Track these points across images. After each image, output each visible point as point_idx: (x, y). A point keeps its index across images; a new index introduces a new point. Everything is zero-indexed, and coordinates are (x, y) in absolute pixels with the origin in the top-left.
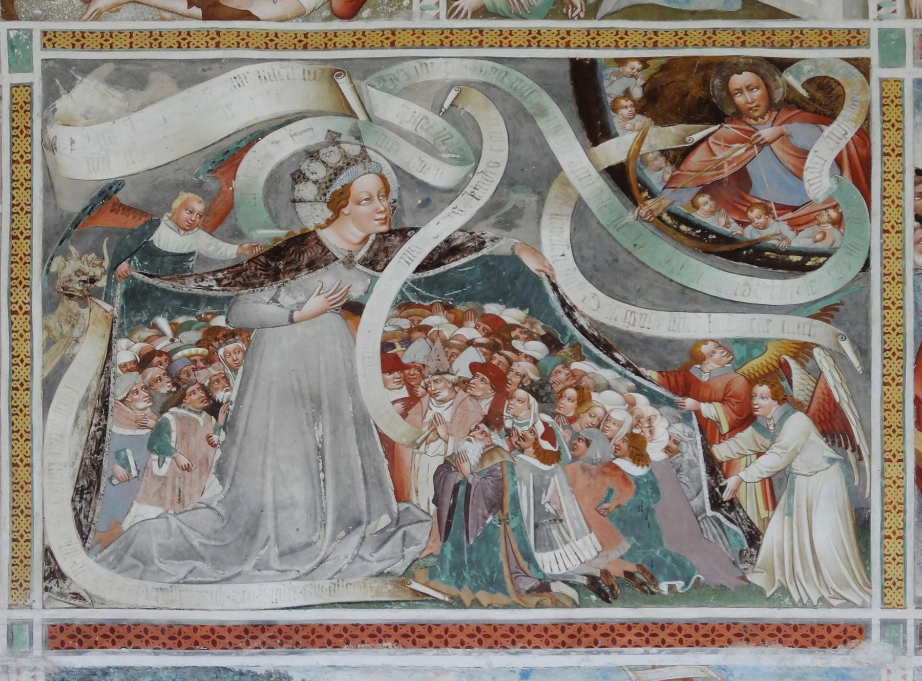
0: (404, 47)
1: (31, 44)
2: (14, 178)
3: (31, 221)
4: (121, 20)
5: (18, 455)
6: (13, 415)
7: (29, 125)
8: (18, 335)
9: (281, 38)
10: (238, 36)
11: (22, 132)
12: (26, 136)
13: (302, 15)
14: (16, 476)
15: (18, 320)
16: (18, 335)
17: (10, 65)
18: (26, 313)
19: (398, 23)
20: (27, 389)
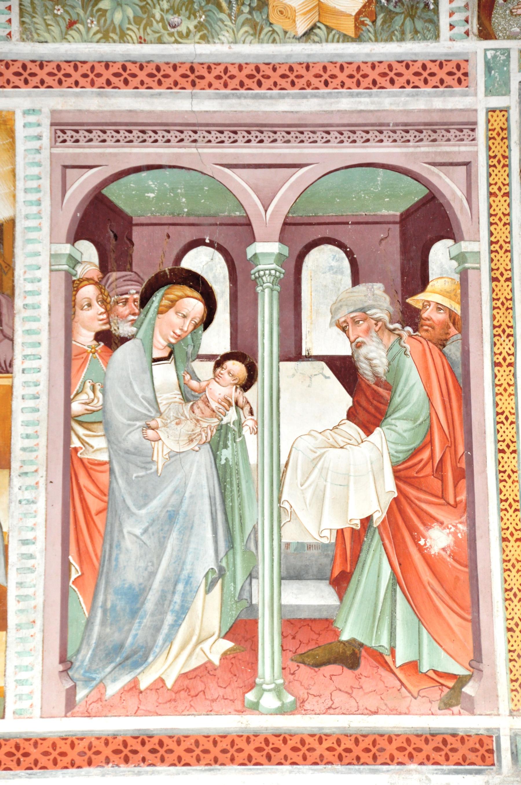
1: (508, 66)
2: (492, 212)
3: (511, 261)
5: (508, 529)
6: (501, 481)
7: (506, 154)
8: (501, 389)
11: (499, 162)
12: (504, 166)
14: (507, 552)
15: (502, 372)
16: (501, 389)
17: (486, 88)
18: (510, 365)
20: (514, 452)
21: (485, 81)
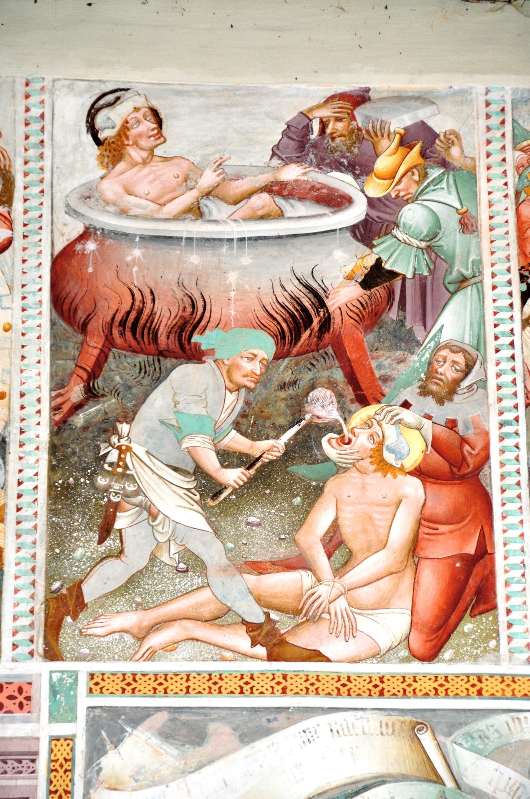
0: (493, 696)
4: (177, 660)
9: (354, 683)
10: (306, 681)
13: (378, 656)
19: (484, 668)
21: (50, 706)
